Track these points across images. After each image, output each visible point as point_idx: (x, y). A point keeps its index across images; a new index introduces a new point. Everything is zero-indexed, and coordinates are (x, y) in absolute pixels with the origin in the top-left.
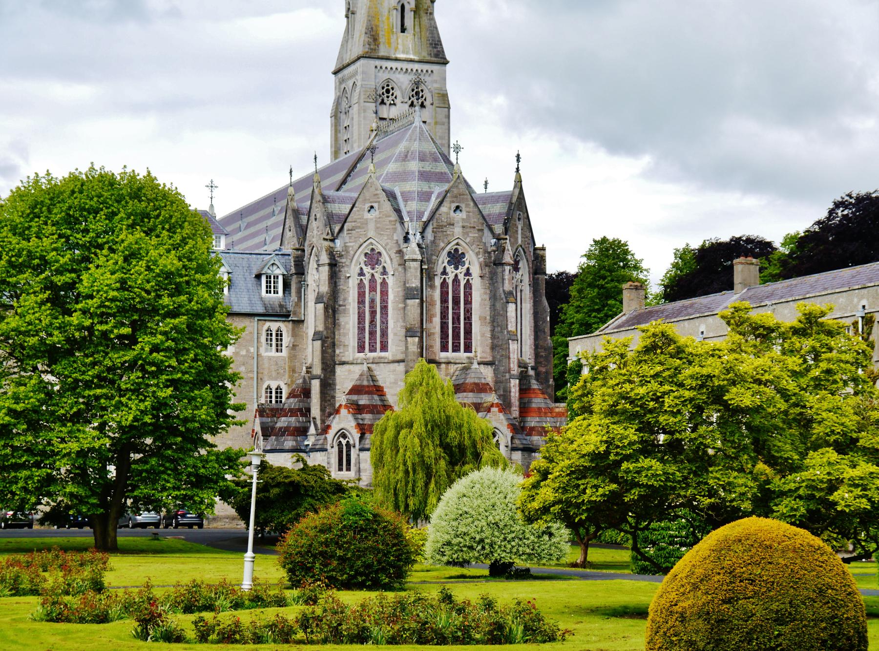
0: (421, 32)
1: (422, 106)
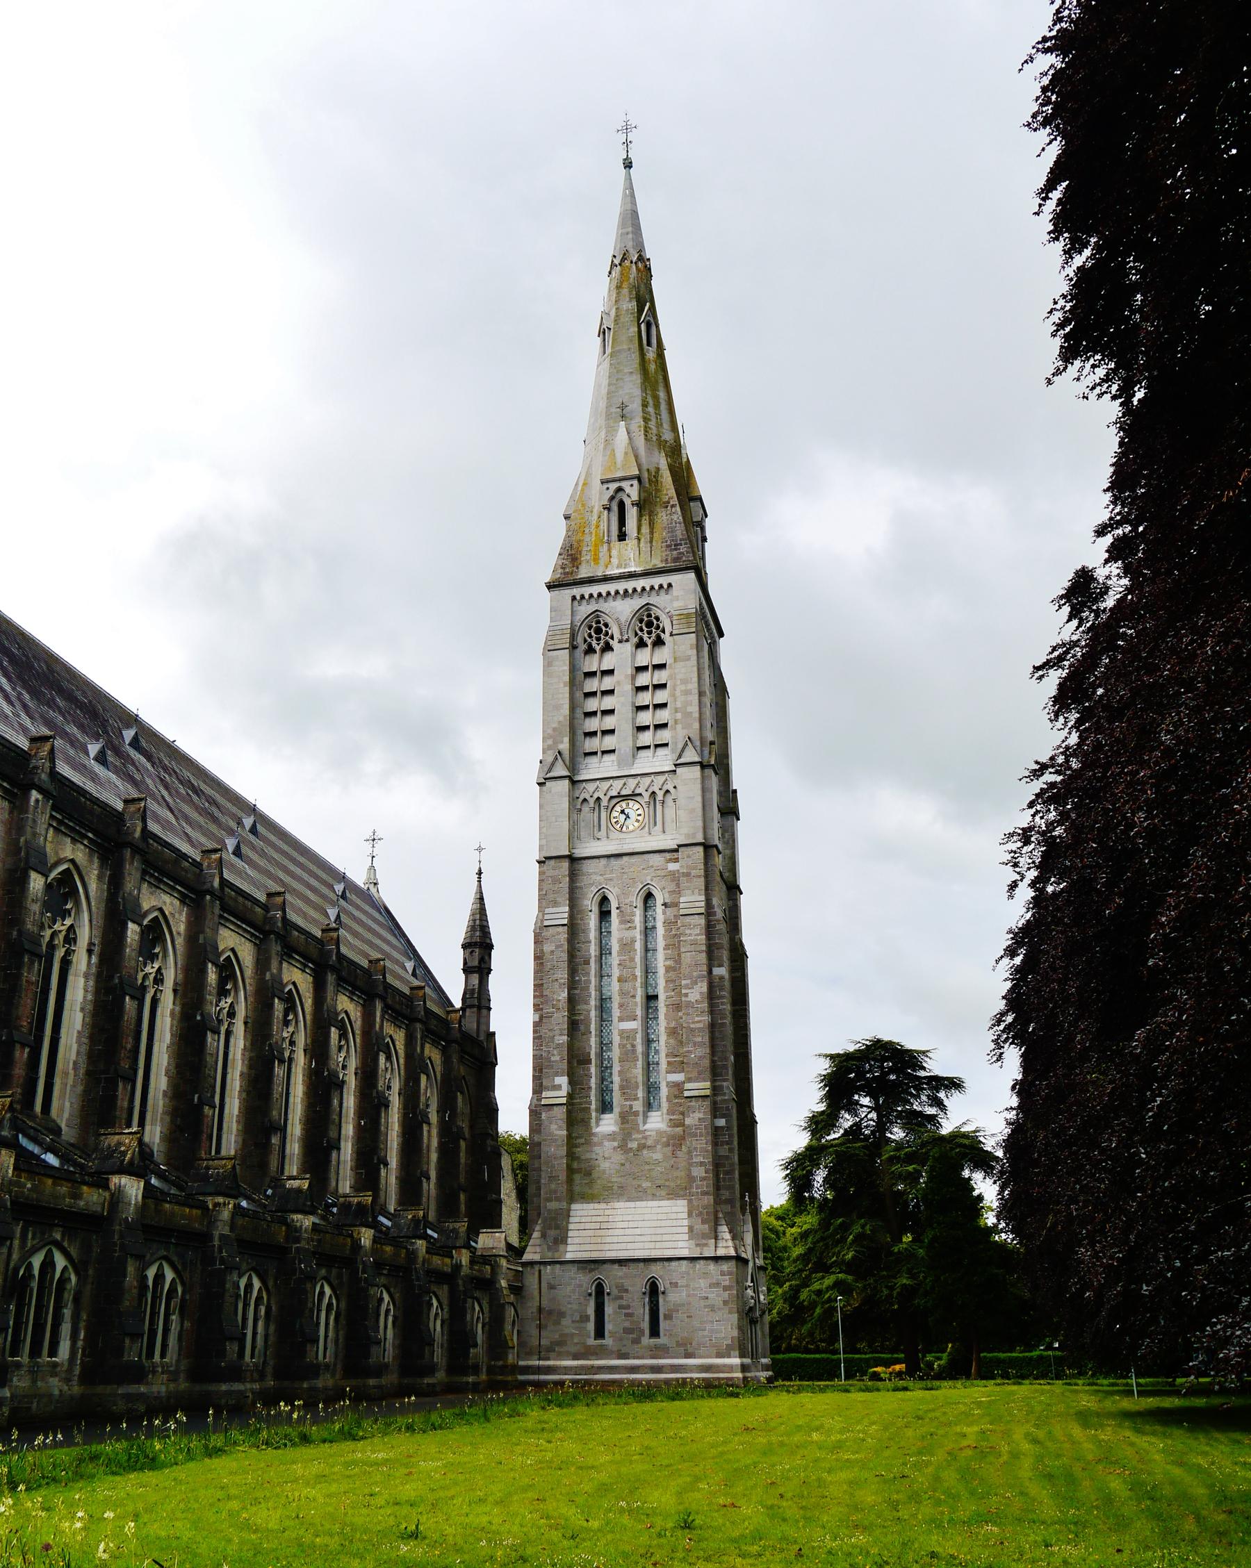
0: (652, 533)
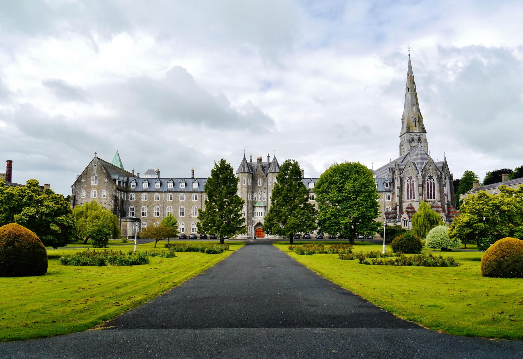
1: (421, 143)
